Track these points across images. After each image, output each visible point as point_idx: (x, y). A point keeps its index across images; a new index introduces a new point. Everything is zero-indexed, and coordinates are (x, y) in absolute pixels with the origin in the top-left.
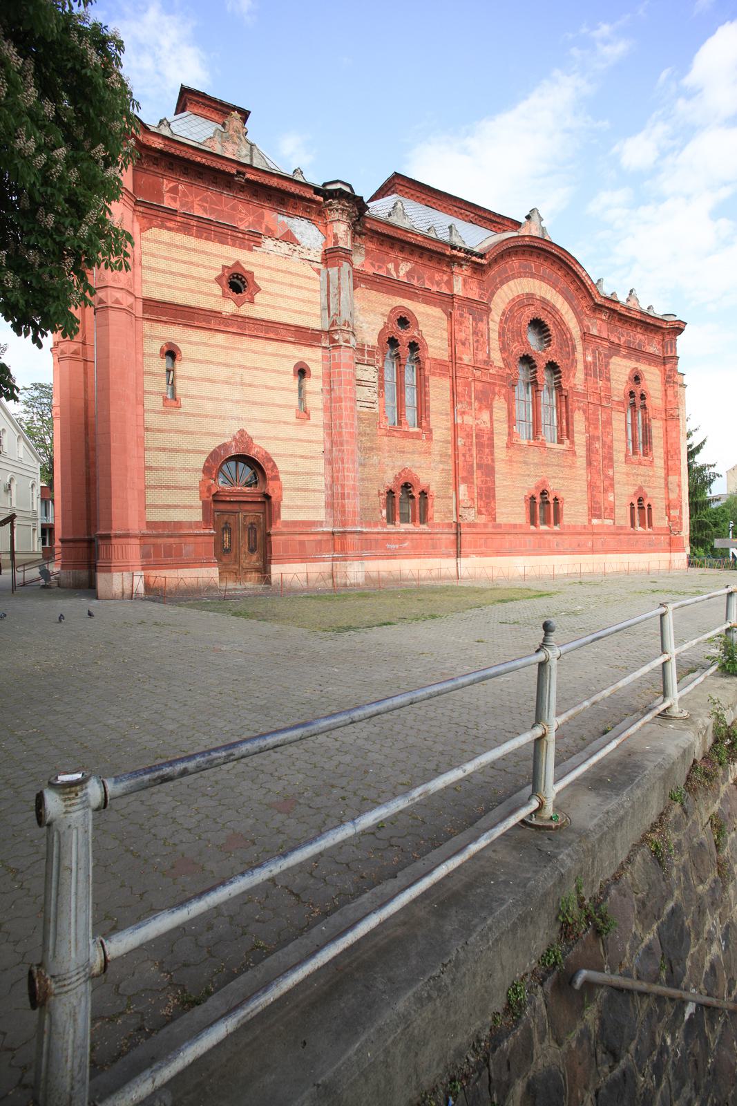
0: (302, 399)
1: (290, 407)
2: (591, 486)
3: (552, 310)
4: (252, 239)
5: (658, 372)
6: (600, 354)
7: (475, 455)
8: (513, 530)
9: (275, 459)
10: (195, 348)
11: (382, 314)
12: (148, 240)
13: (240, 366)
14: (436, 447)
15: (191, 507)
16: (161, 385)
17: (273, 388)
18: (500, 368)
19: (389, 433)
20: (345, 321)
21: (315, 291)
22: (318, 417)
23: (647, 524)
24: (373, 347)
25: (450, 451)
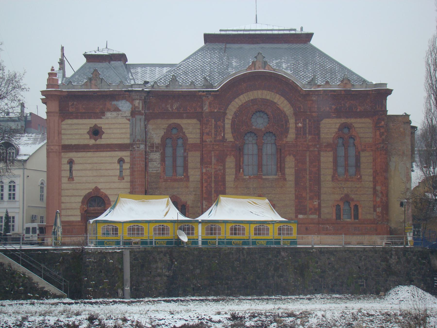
0: (121, 172)
1: (116, 176)
4: (100, 115)
5: (370, 121)
6: (310, 121)
7: (213, 186)
9: (109, 196)
10: (79, 159)
11: (164, 129)
12: (64, 125)
13: (96, 163)
15: (77, 215)
16: (68, 174)
17: (109, 169)
18: (231, 142)
19: (166, 181)
20: (138, 139)
21: (127, 128)
22: (127, 179)
23: (353, 217)
24: (158, 144)
25: (199, 186)
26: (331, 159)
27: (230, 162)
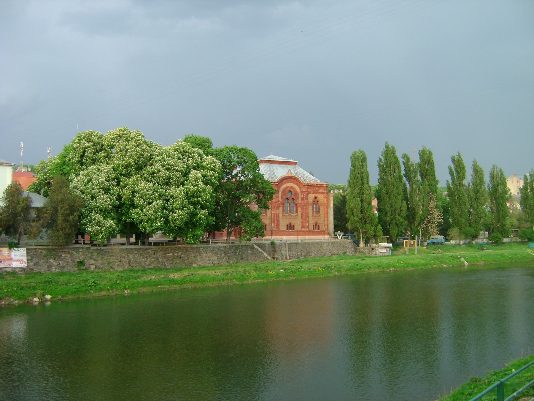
2: (302, 222)
3: (294, 188)
8: (283, 231)
14: (268, 217)
26: (312, 209)
27: (281, 209)
